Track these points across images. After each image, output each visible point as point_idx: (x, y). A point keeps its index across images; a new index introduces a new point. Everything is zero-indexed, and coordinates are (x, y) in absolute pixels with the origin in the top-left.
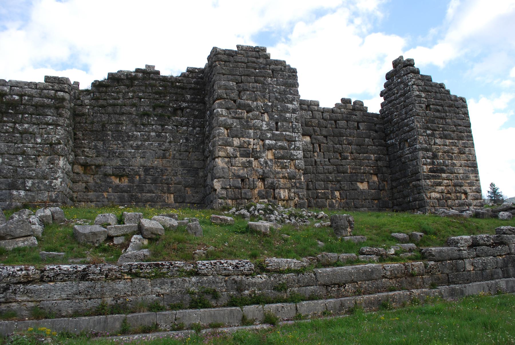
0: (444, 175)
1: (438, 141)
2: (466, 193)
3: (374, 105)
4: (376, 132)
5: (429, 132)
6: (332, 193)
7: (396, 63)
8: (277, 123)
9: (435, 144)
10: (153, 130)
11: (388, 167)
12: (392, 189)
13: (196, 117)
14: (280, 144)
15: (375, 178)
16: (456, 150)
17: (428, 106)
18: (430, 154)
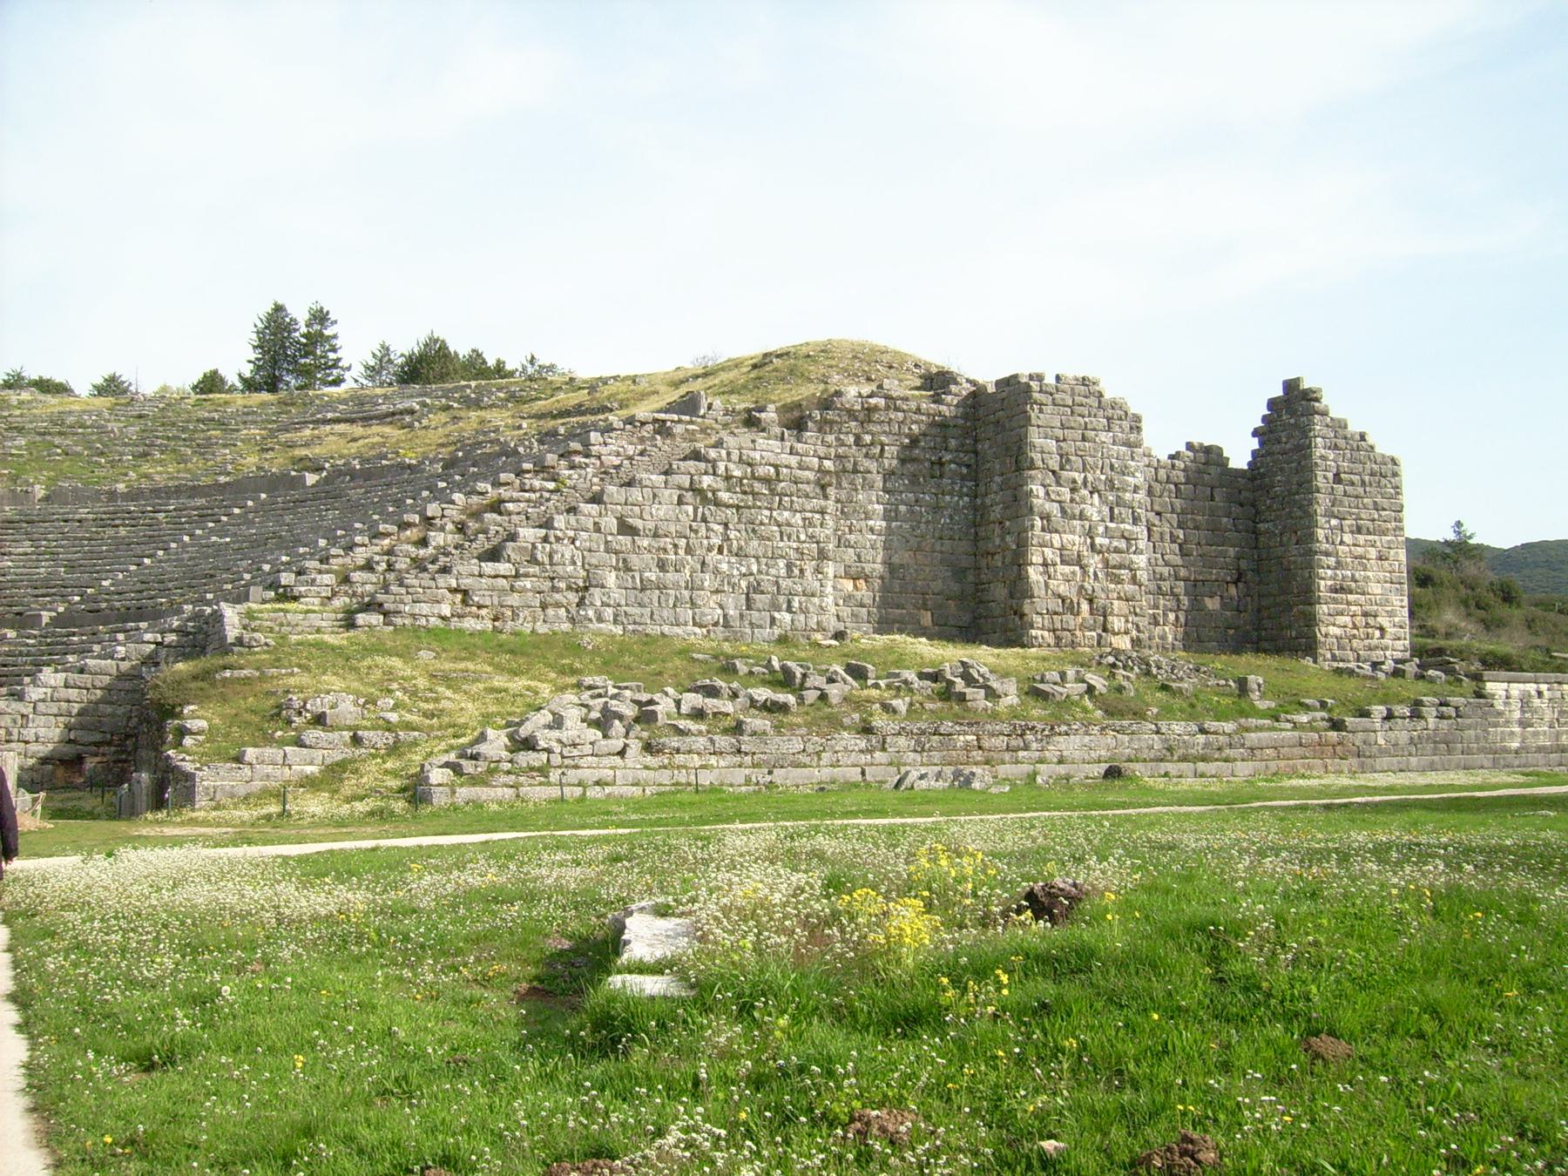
0: (1351, 597)
1: (1347, 538)
2: (1382, 629)
3: (1240, 455)
4: (1241, 505)
5: (1334, 522)
6: (1165, 615)
7: (1291, 386)
8: (1111, 509)
9: (1342, 543)
10: (903, 502)
11: (1257, 571)
12: (1259, 611)
13: (963, 478)
14: (1115, 544)
15: (1233, 590)
16: (1373, 553)
17: (1337, 475)
18: (1332, 561)
